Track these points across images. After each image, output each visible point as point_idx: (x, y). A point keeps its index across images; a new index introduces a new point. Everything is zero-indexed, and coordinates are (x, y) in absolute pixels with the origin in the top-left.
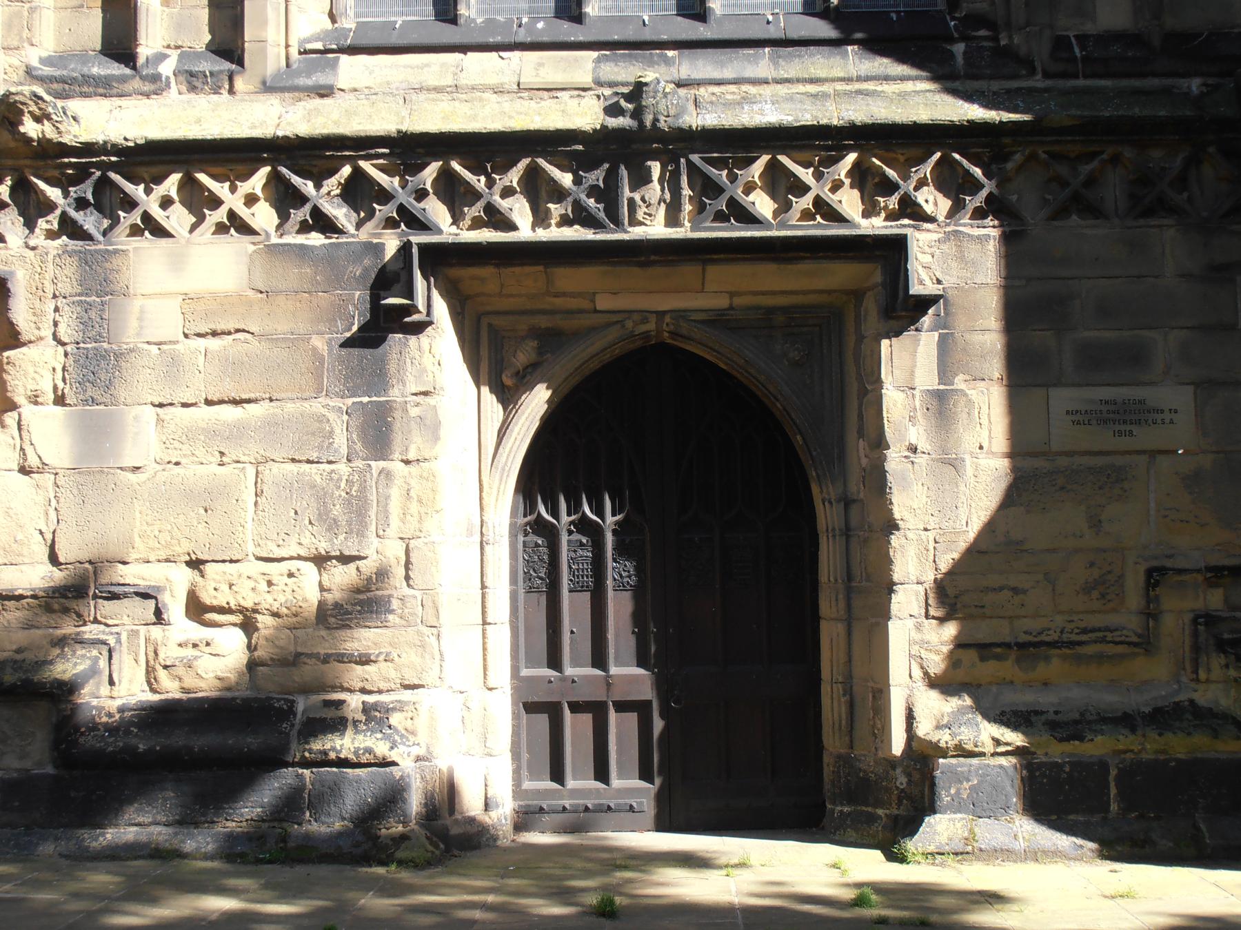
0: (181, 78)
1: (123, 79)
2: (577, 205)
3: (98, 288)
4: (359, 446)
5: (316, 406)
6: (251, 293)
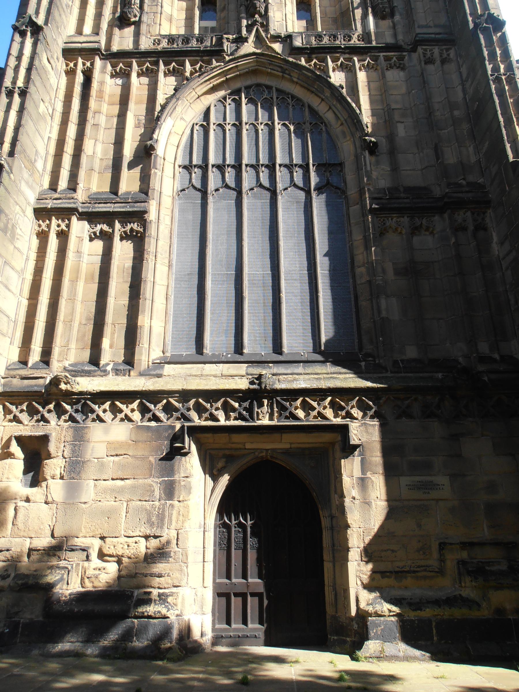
0: (113, 371)
1: (95, 371)
2: (240, 413)
3: (79, 439)
4: (163, 495)
5: (149, 481)
6: (130, 441)
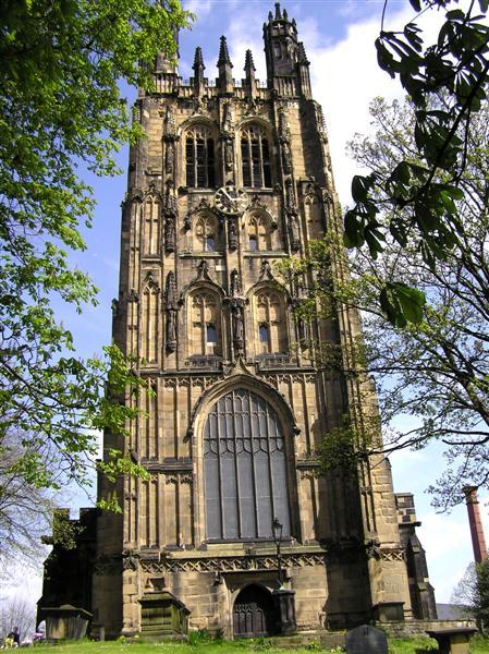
3: (176, 579)
